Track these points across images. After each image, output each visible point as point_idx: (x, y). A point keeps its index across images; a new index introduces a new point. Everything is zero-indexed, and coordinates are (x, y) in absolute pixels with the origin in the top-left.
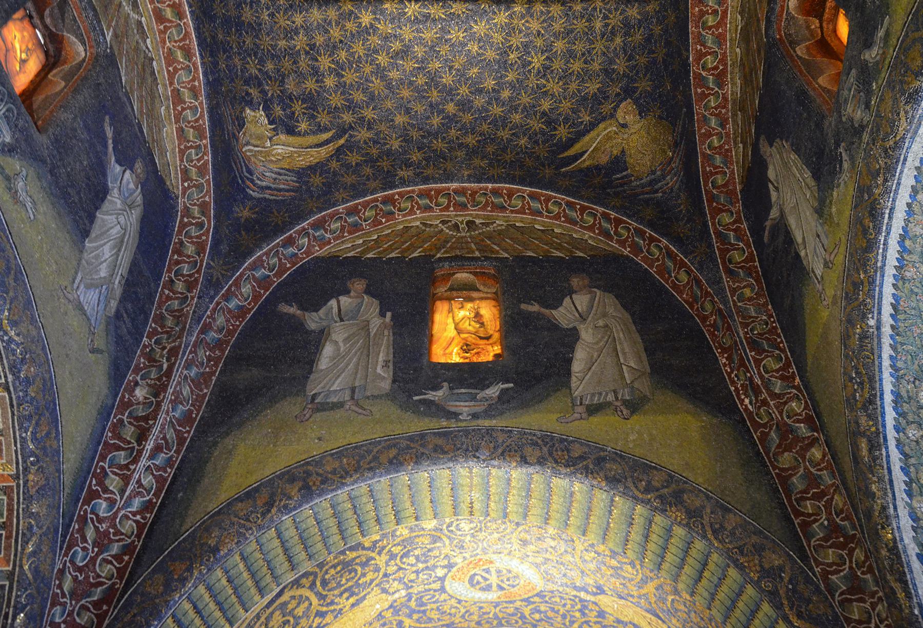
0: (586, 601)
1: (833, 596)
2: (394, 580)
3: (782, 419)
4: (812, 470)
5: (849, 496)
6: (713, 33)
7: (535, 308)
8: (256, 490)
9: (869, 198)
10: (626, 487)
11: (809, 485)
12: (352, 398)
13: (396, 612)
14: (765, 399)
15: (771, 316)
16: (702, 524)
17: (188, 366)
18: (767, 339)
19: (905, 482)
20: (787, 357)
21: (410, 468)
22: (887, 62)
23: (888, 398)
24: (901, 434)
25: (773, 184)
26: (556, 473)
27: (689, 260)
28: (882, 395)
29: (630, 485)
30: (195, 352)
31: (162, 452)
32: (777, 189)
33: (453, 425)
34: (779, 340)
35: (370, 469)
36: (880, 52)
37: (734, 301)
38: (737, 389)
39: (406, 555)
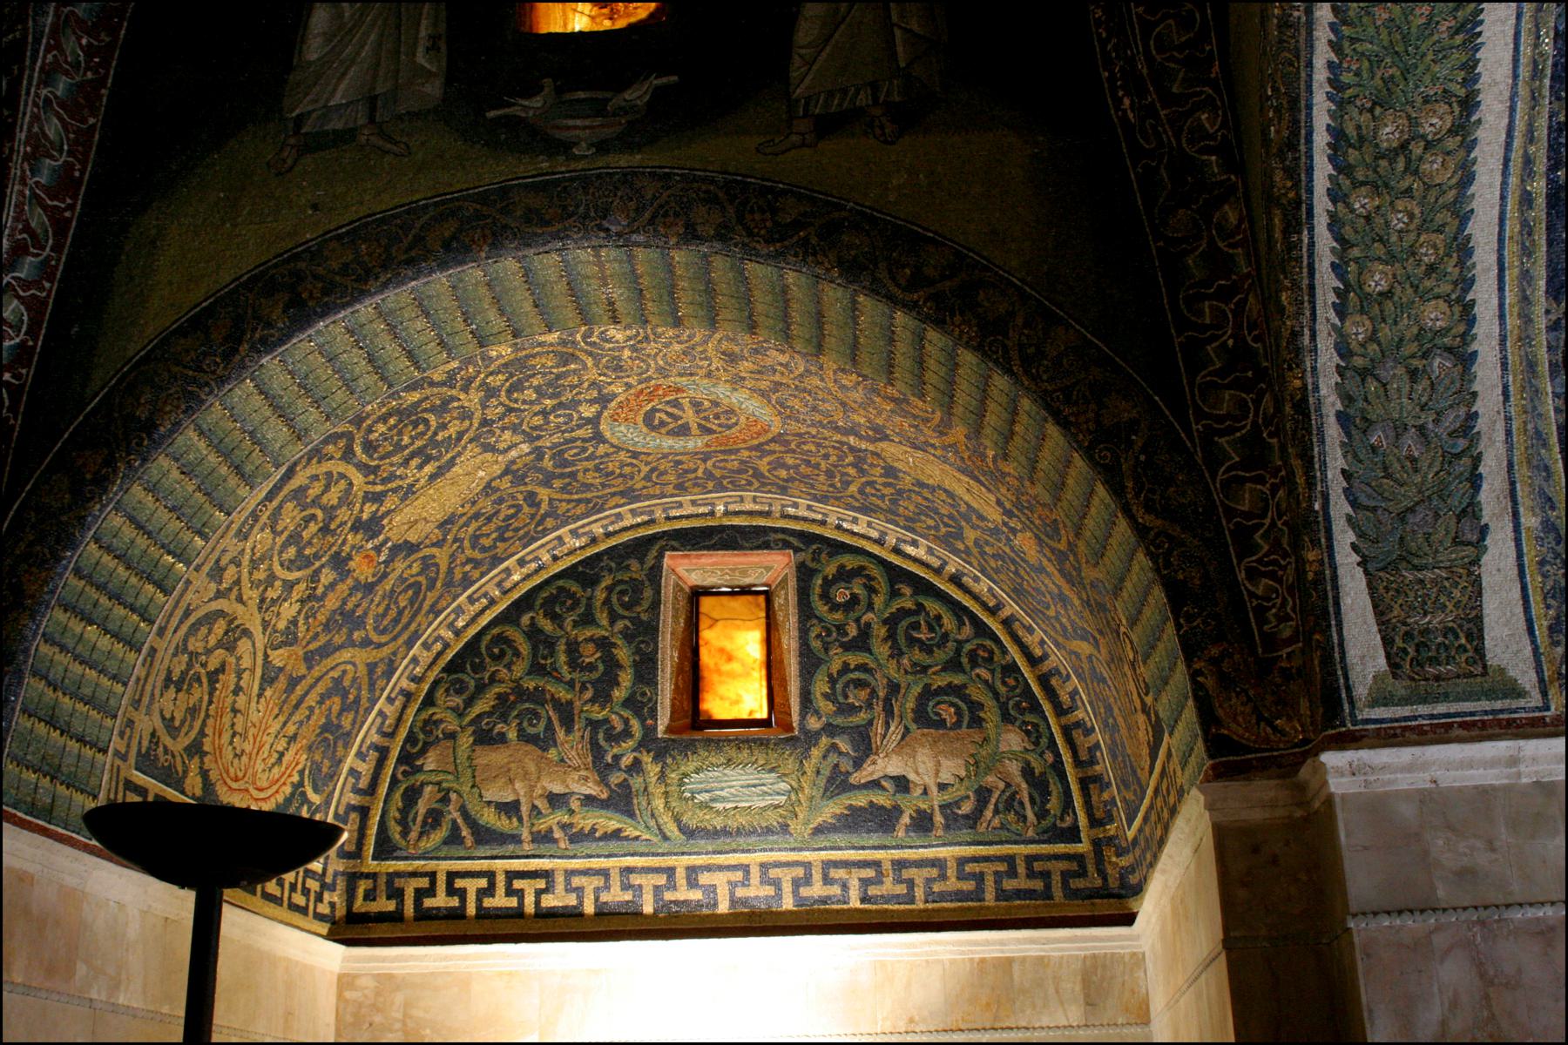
0: (860, 450)
2: (503, 429)
4: (1220, 244)
8: (209, 312)
10: (875, 280)
12: (372, 120)
13: (519, 479)
16: (1005, 346)
17: (48, 78)
19: (1335, 290)
21: (483, 255)
23: (1321, 139)
24: (1340, 205)
26: (751, 254)
28: (1310, 134)
29: (883, 274)
30: (58, 47)
31: (29, 254)
33: (561, 167)
35: (410, 262)
38: (1112, 73)
39: (516, 387)
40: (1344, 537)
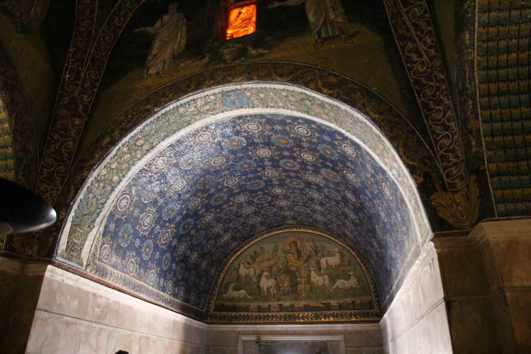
1: (40, 176)
4: (70, 125)
9: (203, 80)
14: (78, 84)
15: (106, 56)
20: (99, 77)
22: (254, 60)
25: (162, 22)
32: (162, 26)
36: (255, 55)
40: (72, 214)
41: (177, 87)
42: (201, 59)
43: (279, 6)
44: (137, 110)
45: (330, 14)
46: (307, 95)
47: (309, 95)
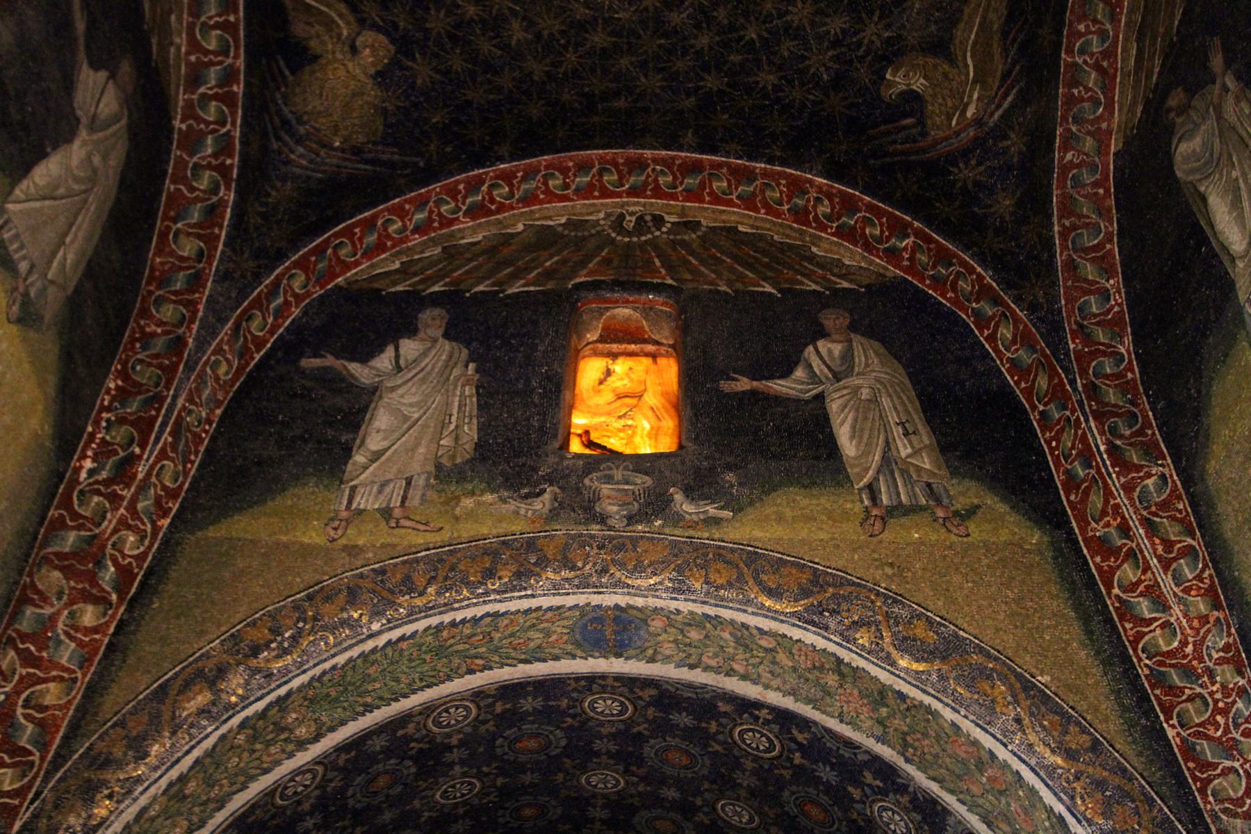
3: (108, 539)
4: (60, 625)
5: (82, 710)
6: (538, 188)
7: (80, 26)
9: (535, 564)
11: (34, 634)
18: (187, 441)
20: (183, 483)
22: (691, 533)
23: (282, 691)
25: (397, 357)
27: (223, 252)
32: (399, 368)
34: (193, 457)
36: (695, 518)
37: (209, 358)
41: (452, 569)
42: (527, 497)
43: (753, 392)
44: (315, 619)
45: (898, 442)
46: (839, 661)
47: (713, 614)
